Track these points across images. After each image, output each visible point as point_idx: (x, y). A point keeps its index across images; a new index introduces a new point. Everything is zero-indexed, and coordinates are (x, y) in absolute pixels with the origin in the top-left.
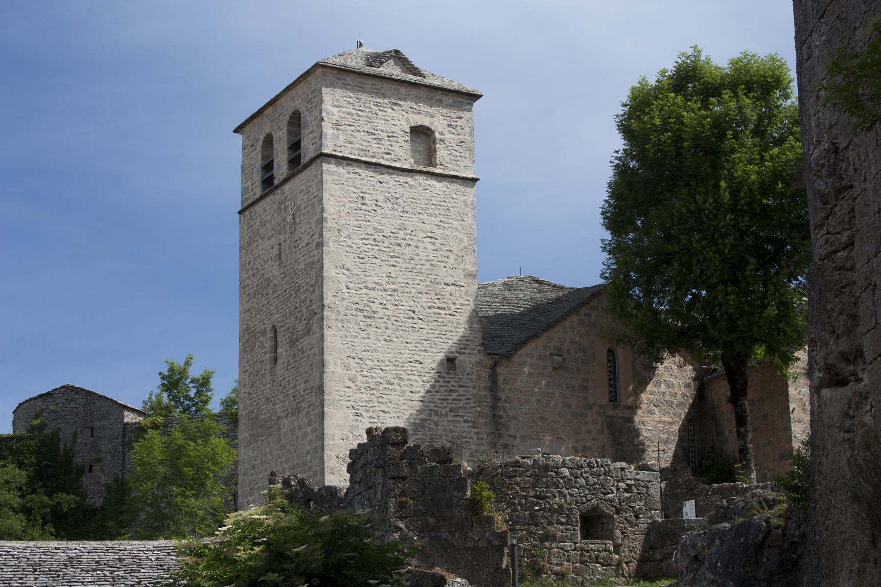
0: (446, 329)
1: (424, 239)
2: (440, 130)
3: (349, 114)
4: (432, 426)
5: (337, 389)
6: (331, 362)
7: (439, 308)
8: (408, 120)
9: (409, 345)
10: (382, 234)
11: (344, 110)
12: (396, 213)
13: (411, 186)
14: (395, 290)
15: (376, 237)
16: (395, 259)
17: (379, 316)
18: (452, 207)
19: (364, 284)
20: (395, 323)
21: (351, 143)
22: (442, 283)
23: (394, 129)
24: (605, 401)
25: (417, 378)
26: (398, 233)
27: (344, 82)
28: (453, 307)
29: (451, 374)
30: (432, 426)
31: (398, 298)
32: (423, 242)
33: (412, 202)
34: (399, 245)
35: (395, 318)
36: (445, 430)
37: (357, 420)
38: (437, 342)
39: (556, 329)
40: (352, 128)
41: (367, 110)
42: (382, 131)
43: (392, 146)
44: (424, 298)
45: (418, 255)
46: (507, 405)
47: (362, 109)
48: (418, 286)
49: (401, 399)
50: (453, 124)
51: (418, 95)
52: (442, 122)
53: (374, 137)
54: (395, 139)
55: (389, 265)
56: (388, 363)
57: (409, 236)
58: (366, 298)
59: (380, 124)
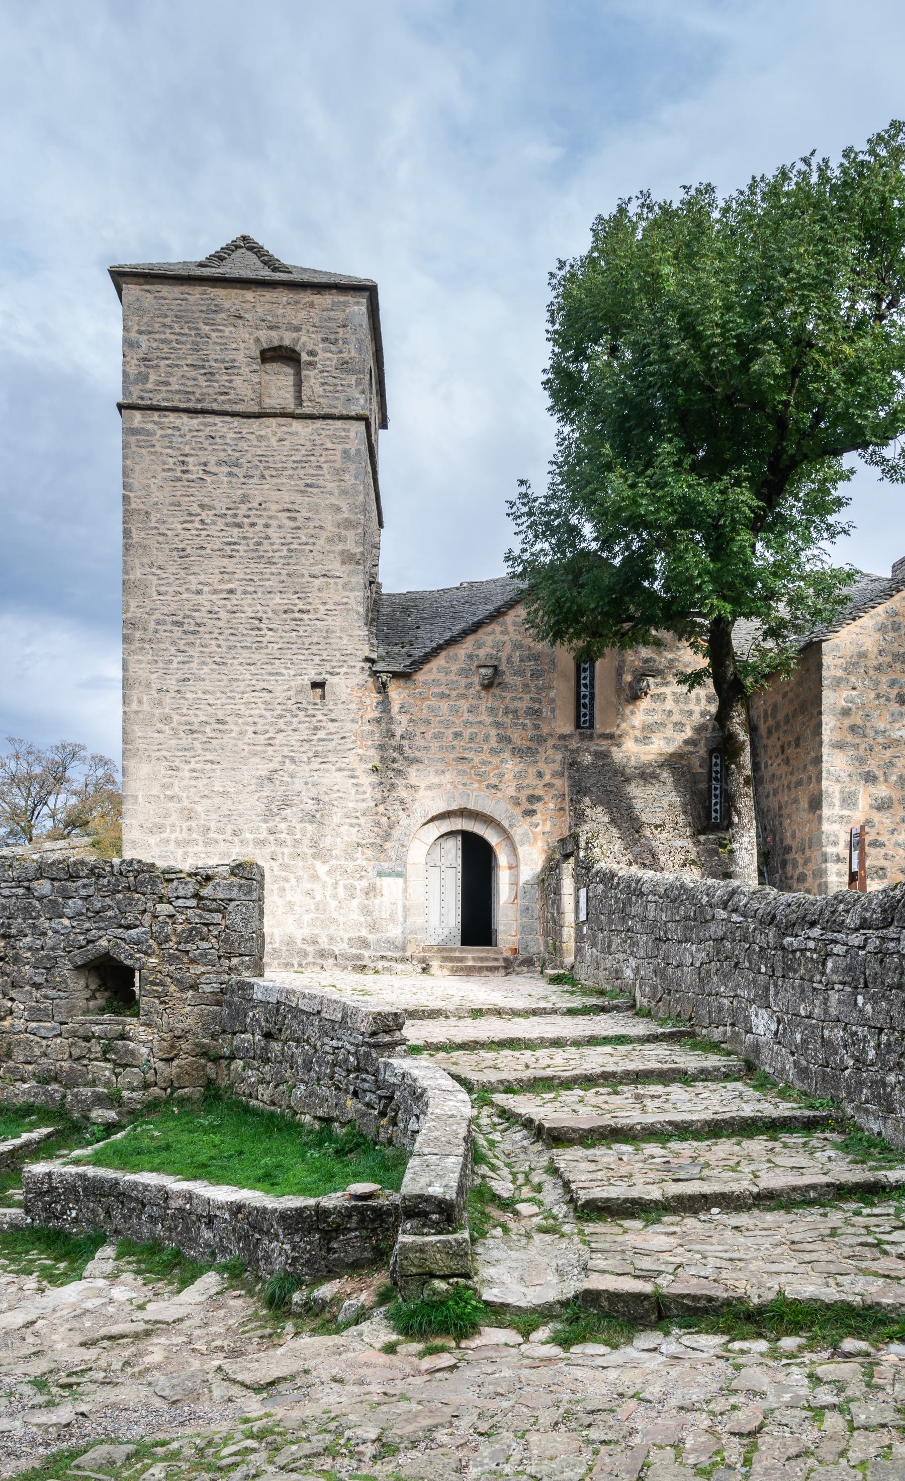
0: (309, 640)
1: (280, 514)
2: (310, 347)
3: (163, 341)
4: (286, 779)
5: (140, 734)
6: (135, 698)
7: (300, 611)
8: (257, 340)
9: (252, 668)
10: (213, 512)
11: (157, 336)
12: (234, 480)
13: (260, 438)
14: (231, 592)
15: (204, 517)
16: (233, 547)
17: (207, 629)
18: (326, 462)
19: (185, 586)
20: (231, 638)
21: (167, 384)
22: (307, 575)
23: (232, 355)
24: (568, 728)
25: (263, 712)
26: (237, 509)
27: (157, 295)
28: (322, 608)
29: (316, 704)
30: (286, 779)
31: (236, 602)
32: (276, 517)
33: (260, 461)
34: (239, 526)
35: (232, 631)
36: (306, 783)
37: (171, 776)
38: (295, 661)
39: (490, 628)
40: (167, 362)
41: (193, 333)
42: (216, 361)
43: (231, 381)
44: (277, 599)
45: (268, 538)
46: (405, 743)
47: (186, 331)
48: (268, 583)
49: (240, 743)
50: (332, 337)
51: (274, 300)
52: (313, 336)
53: (203, 371)
54: (236, 371)
55: (224, 556)
56: (218, 695)
57: (254, 512)
58: (188, 606)
59: (213, 353)
